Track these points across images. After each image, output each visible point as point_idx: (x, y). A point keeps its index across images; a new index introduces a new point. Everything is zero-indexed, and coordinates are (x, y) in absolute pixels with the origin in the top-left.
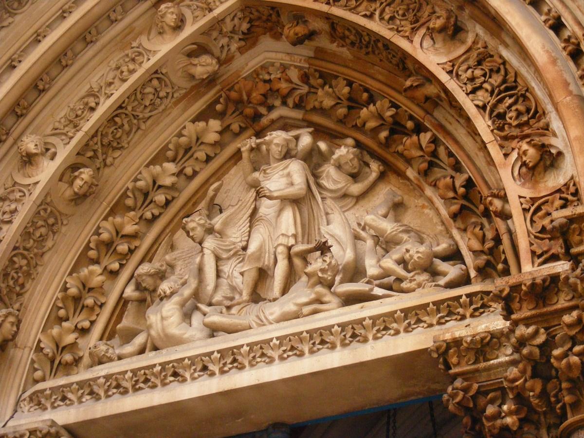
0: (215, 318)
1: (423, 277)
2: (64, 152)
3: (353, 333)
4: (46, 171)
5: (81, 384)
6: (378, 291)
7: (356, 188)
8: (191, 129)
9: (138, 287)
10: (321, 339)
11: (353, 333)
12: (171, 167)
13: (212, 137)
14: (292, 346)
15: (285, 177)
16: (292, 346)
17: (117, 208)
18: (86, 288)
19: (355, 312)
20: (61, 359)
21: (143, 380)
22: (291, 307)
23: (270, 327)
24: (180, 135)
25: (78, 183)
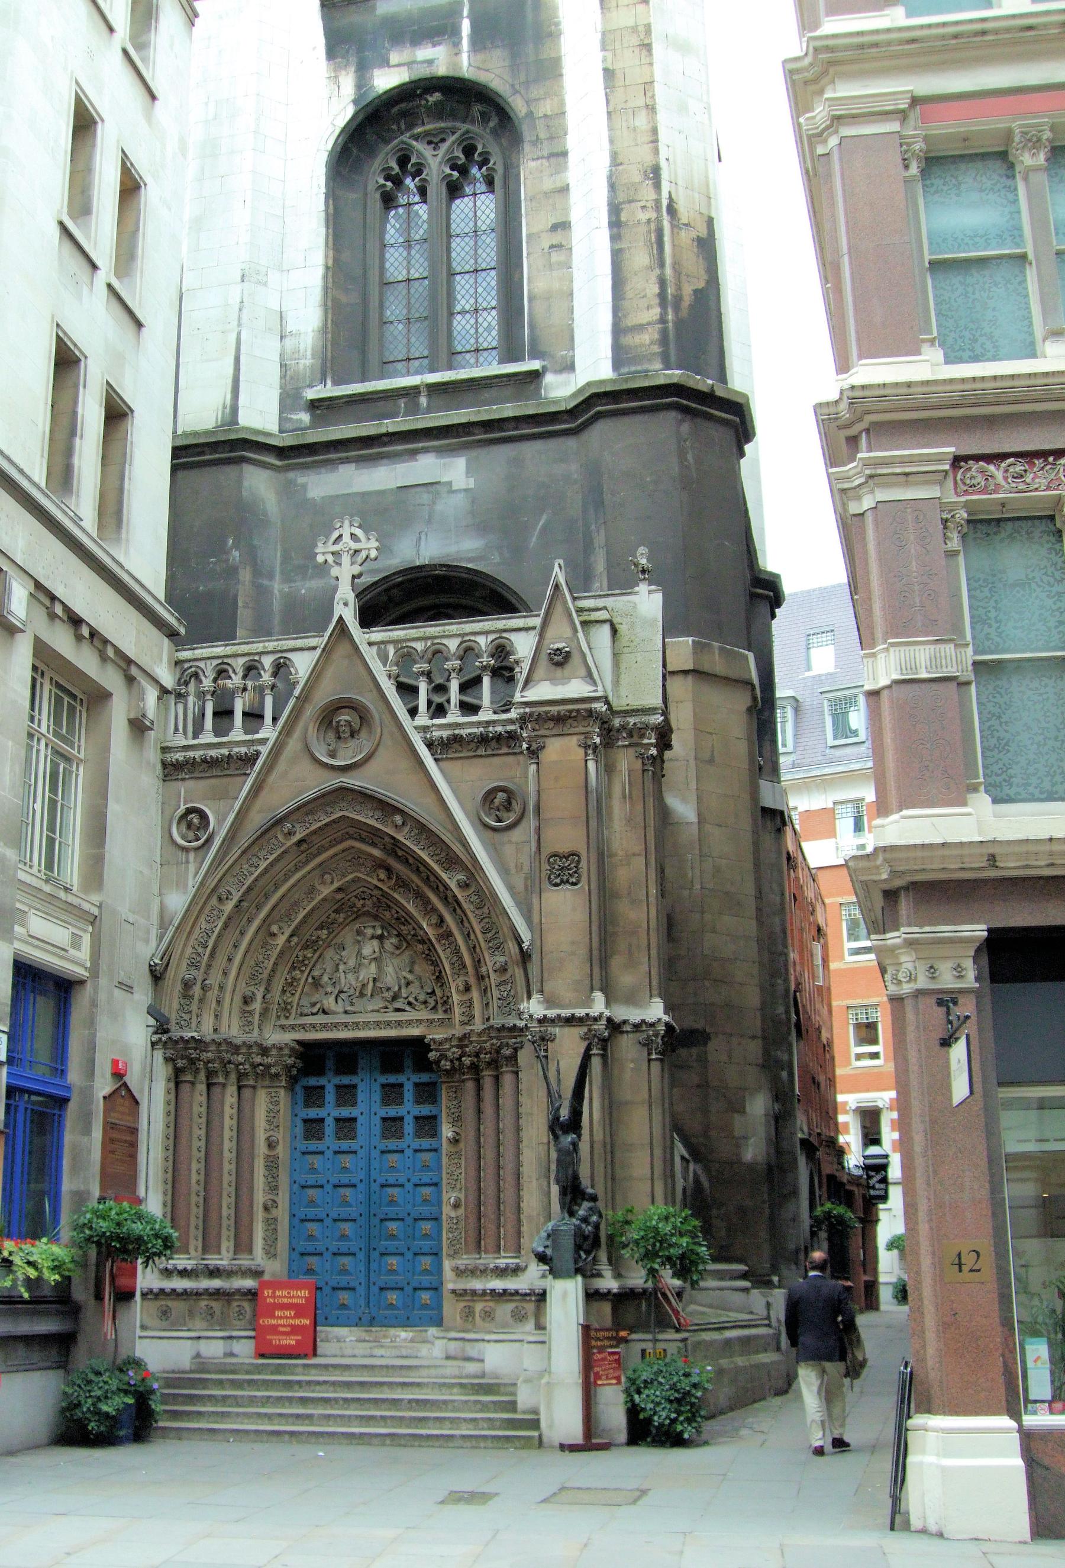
0: (349, 1008)
1: (423, 1006)
2: (288, 932)
3: (399, 1024)
4: (281, 940)
5: (300, 1025)
6: (408, 1008)
7: (398, 952)
8: (333, 915)
9: (313, 978)
10: (388, 1024)
11: (399, 1024)
12: (325, 932)
13: (341, 920)
14: (378, 1024)
15: (370, 948)
16: (378, 1024)
17: (306, 947)
18: (294, 979)
19: (399, 1016)
20: (285, 1008)
21: (325, 1027)
22: (376, 1008)
23: (370, 1015)
24: (328, 918)
25: (293, 943)
